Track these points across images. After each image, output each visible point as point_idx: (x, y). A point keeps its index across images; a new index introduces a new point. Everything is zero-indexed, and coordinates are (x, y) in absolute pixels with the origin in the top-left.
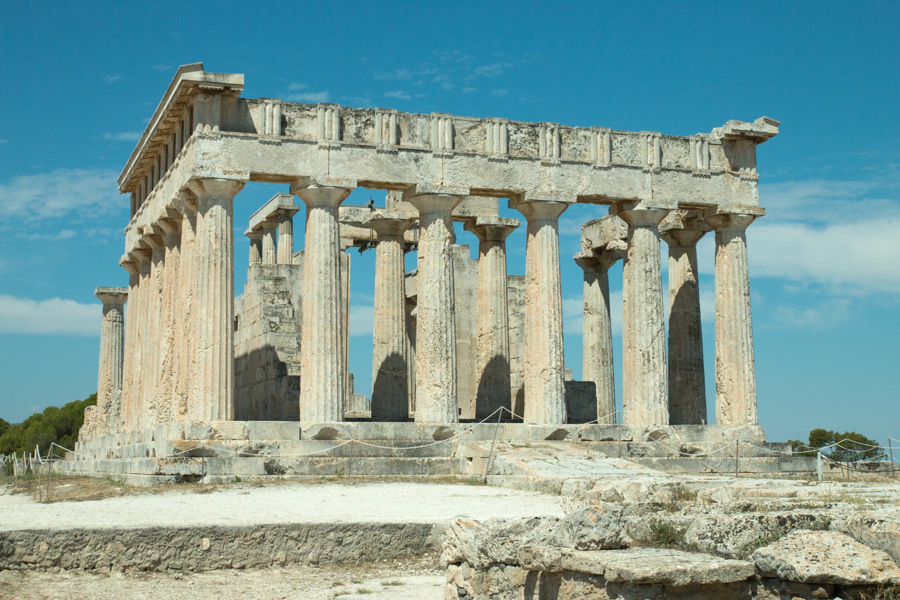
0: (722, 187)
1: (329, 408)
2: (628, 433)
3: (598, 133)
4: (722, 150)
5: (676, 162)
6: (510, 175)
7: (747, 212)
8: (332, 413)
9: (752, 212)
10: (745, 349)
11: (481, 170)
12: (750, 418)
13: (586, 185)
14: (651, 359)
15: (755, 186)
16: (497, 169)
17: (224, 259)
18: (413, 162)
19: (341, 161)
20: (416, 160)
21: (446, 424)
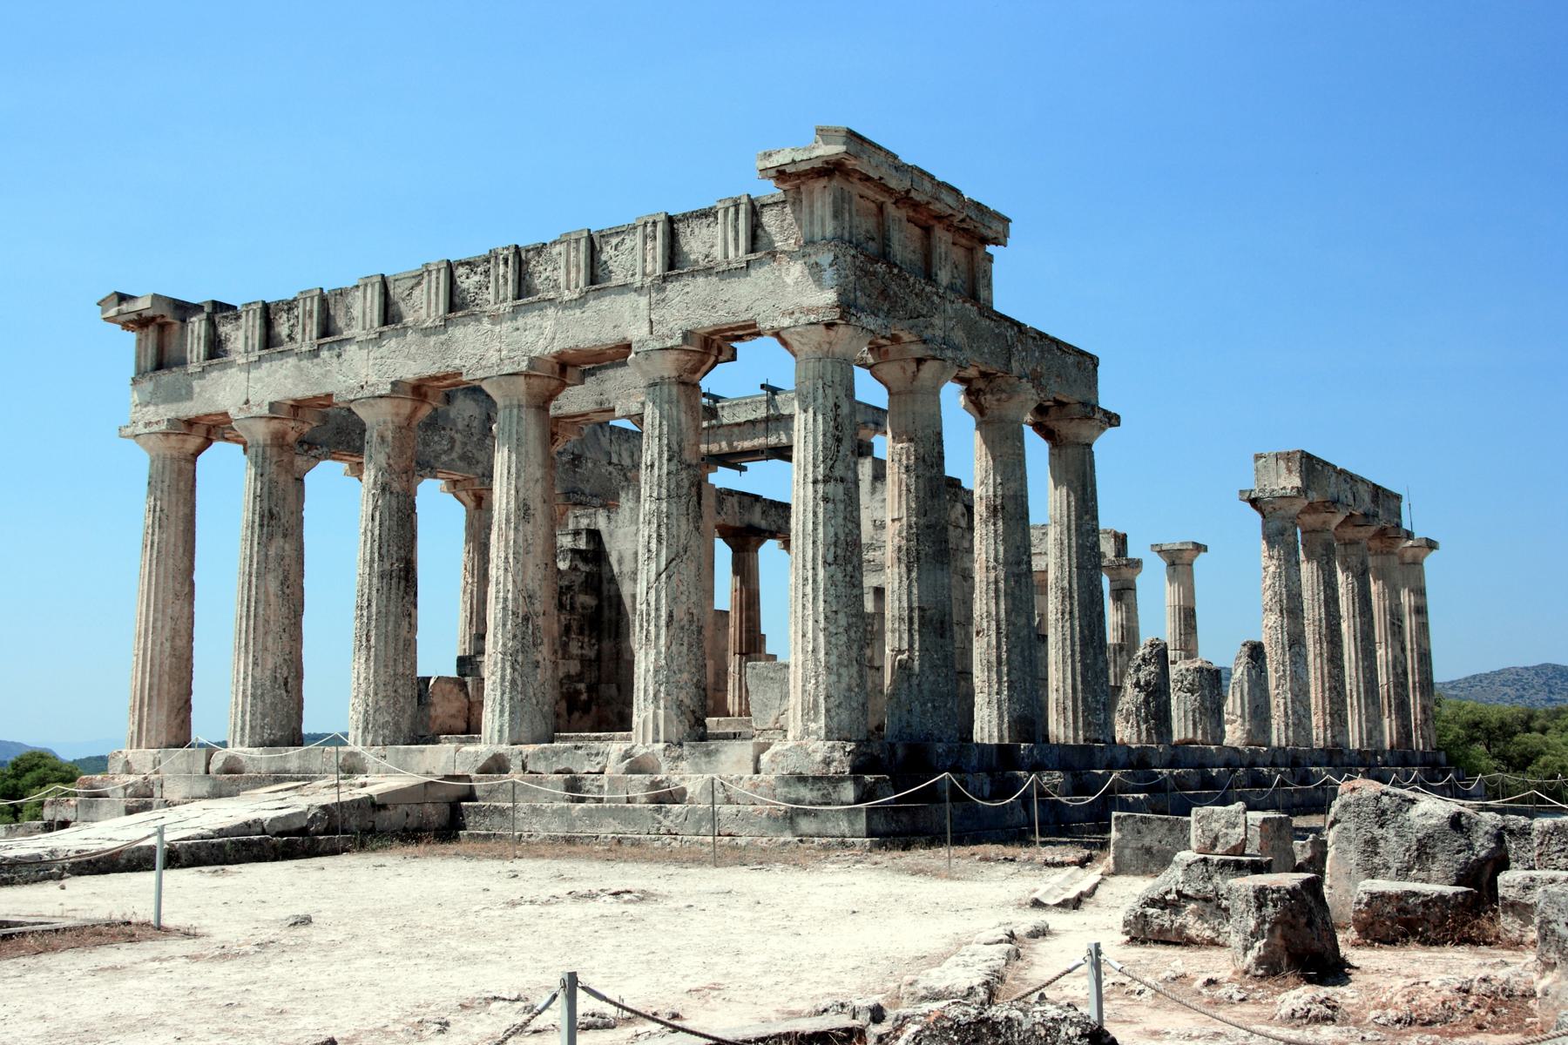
0: (769, 283)
1: (238, 729)
2: (599, 759)
3: (569, 245)
4: (788, 210)
5: (707, 256)
6: (448, 348)
7: (803, 320)
8: (242, 736)
9: (812, 318)
10: (809, 589)
11: (413, 349)
12: (813, 726)
13: (550, 336)
14: (645, 624)
15: (831, 265)
16: (432, 343)
17: (156, 537)
18: (335, 359)
19: (260, 379)
20: (339, 356)
21: (359, 748)
